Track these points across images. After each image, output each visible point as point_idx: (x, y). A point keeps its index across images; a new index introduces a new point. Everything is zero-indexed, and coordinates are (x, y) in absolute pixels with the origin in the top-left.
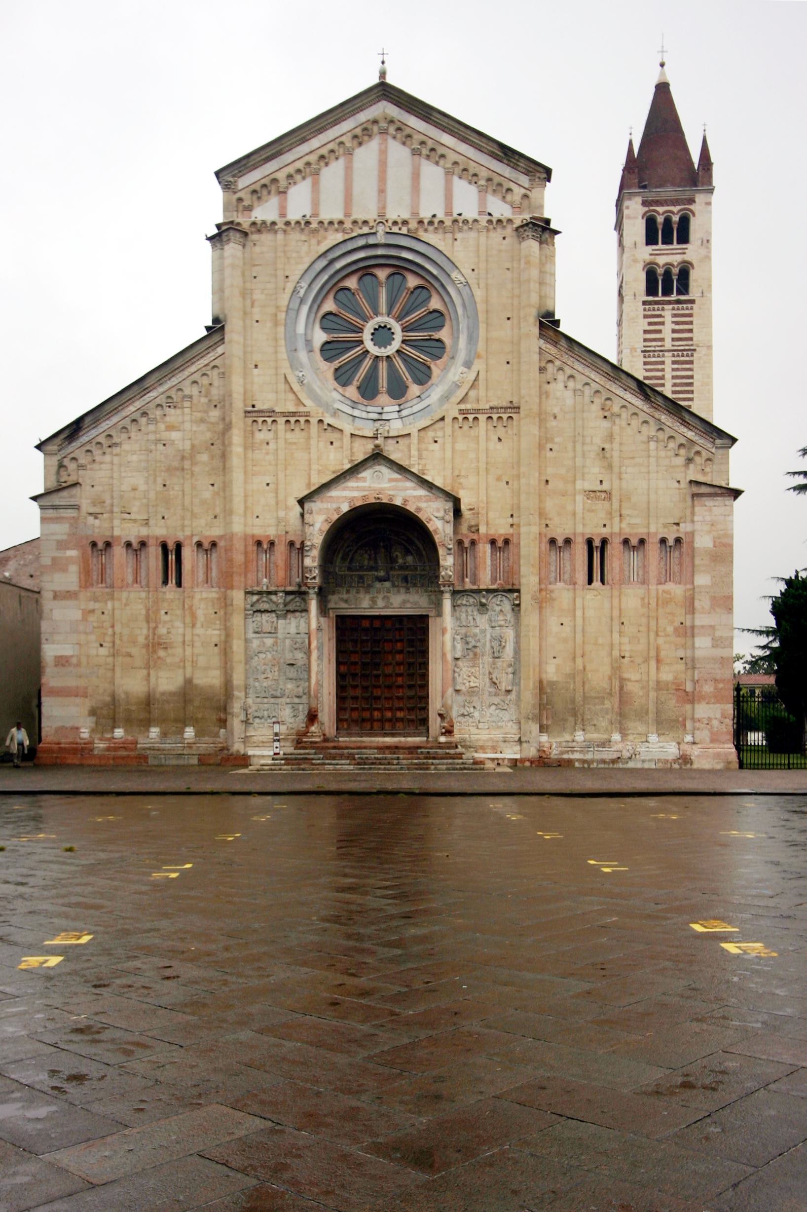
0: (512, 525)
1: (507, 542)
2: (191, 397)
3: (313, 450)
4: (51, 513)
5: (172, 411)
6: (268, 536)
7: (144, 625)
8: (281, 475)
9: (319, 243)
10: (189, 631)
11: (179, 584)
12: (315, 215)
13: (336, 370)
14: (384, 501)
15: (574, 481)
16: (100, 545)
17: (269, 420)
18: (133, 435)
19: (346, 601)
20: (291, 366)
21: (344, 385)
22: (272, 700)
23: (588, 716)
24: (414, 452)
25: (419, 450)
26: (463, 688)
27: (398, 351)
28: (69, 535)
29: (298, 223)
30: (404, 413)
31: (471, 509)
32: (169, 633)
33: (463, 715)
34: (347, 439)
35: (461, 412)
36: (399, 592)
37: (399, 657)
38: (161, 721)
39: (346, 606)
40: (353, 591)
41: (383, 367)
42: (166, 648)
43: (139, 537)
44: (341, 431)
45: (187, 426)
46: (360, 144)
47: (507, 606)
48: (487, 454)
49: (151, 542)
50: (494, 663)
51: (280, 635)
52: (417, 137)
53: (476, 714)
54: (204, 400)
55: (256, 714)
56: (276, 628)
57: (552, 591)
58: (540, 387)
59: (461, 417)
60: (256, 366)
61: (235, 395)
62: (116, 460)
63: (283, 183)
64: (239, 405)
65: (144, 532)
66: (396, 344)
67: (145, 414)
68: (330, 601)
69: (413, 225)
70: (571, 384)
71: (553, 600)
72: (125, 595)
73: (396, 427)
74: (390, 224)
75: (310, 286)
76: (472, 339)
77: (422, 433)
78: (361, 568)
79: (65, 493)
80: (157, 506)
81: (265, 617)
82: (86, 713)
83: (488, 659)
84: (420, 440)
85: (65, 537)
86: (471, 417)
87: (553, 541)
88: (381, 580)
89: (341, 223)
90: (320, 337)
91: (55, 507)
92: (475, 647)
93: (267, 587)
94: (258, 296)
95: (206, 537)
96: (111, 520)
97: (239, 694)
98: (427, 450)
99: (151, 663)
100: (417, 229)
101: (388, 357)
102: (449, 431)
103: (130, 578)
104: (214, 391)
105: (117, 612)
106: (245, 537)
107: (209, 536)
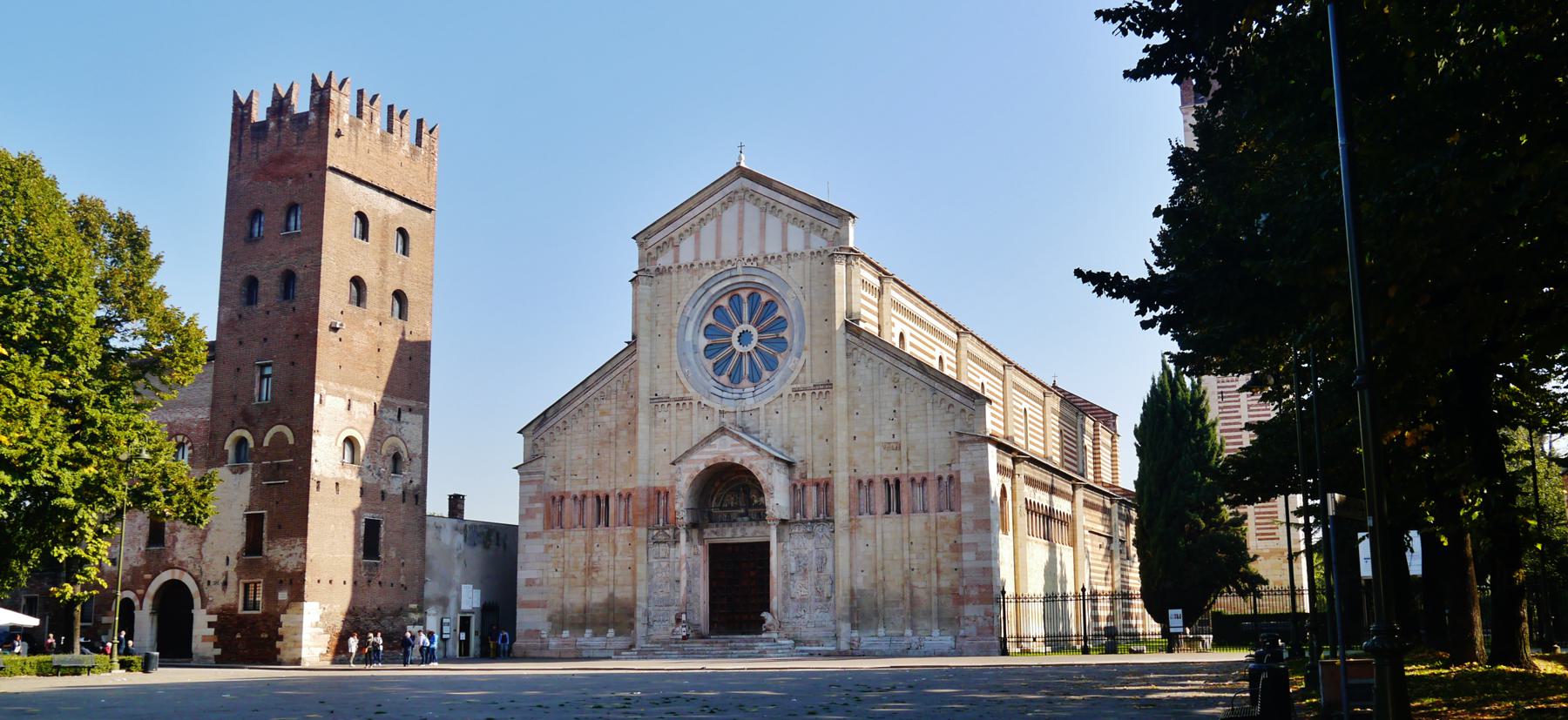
0: (830, 472)
1: (827, 484)
2: (616, 391)
3: (694, 423)
4: (526, 478)
5: (605, 401)
6: (664, 488)
7: (584, 555)
8: (673, 443)
9: (699, 279)
10: (611, 558)
11: (607, 525)
12: (697, 259)
13: (715, 364)
14: (729, 461)
15: (874, 437)
16: (557, 498)
17: (666, 404)
18: (579, 420)
19: (716, 533)
20: (681, 366)
21: (720, 375)
22: (666, 608)
23: (887, 616)
24: (762, 422)
25: (766, 419)
26: (798, 597)
27: (755, 348)
28: (537, 492)
29: (686, 266)
30: (757, 392)
31: (802, 461)
32: (599, 560)
33: (797, 617)
34: (717, 415)
35: (794, 390)
36: (752, 525)
37: (752, 574)
38: (593, 625)
39: (715, 536)
40: (721, 525)
41: (746, 360)
42: (597, 571)
43: (581, 491)
44: (713, 408)
45: (613, 412)
46: (727, 208)
47: (827, 531)
48: (812, 419)
49: (589, 495)
50: (818, 576)
51: (671, 560)
52: (764, 200)
53: (807, 616)
54: (625, 393)
55: (655, 619)
56: (669, 555)
57: (860, 520)
58: (848, 368)
59: (794, 394)
60: (658, 367)
61: (641, 389)
62: (568, 438)
63: (676, 240)
64: (644, 395)
65: (585, 488)
66: (754, 343)
67: (587, 405)
68: (703, 533)
69: (760, 262)
70: (870, 364)
71: (861, 527)
72: (572, 533)
73: (750, 403)
74: (746, 259)
75: (694, 307)
76: (802, 337)
77: (767, 407)
78: (729, 507)
79: (534, 464)
80: (593, 469)
81: (662, 546)
82: (546, 619)
83: (813, 574)
84: (767, 412)
85: (534, 494)
86: (801, 393)
87: (860, 482)
88: (741, 515)
89: (714, 263)
90: (703, 342)
91: (529, 474)
92: (805, 565)
93: (663, 525)
94: (660, 318)
95: (624, 490)
96: (565, 481)
97: (642, 605)
98: (770, 419)
99: (589, 582)
100: (763, 264)
101: (749, 352)
102: (785, 404)
103: (577, 522)
104: (631, 386)
105: (567, 546)
106: (648, 489)
107: (627, 489)
